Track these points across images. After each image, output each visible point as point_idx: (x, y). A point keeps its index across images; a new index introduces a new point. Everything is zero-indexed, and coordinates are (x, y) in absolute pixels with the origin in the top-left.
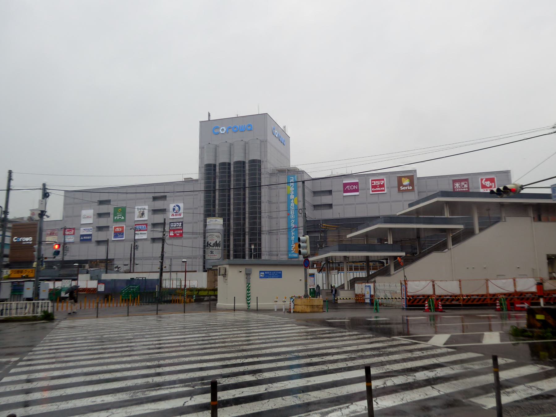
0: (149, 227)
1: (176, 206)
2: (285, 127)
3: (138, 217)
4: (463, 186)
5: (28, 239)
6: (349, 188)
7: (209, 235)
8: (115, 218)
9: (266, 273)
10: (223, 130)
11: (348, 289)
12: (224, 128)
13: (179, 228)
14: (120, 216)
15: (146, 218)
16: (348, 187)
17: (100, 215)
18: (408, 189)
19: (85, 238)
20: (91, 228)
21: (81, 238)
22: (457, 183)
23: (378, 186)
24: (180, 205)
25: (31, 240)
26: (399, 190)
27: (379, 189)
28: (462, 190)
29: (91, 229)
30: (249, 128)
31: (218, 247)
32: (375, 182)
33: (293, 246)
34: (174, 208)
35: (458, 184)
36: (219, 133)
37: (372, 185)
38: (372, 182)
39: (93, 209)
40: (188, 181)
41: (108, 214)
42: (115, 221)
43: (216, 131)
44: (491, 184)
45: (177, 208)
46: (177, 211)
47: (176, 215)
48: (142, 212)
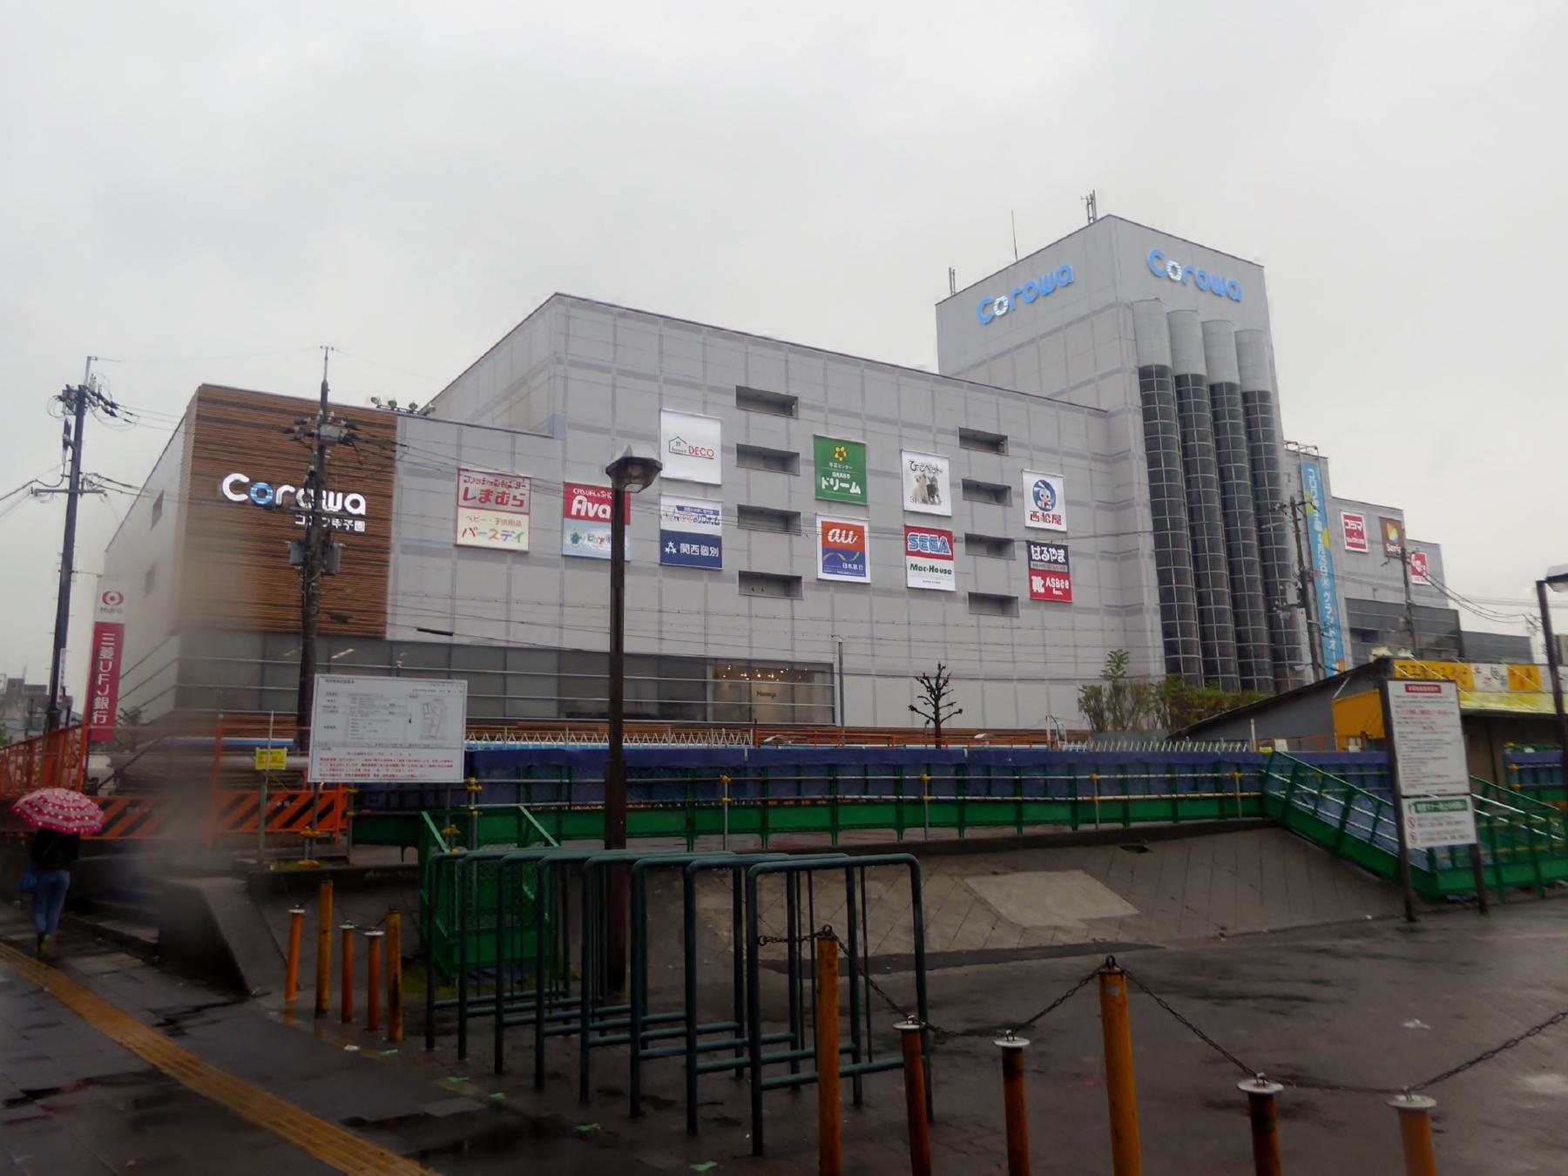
3: (915, 500)
13: (1054, 567)
14: (842, 480)
19: (685, 548)
20: (718, 508)
25: (362, 510)
29: (716, 513)
34: (1036, 489)
42: (827, 498)
46: (1046, 504)
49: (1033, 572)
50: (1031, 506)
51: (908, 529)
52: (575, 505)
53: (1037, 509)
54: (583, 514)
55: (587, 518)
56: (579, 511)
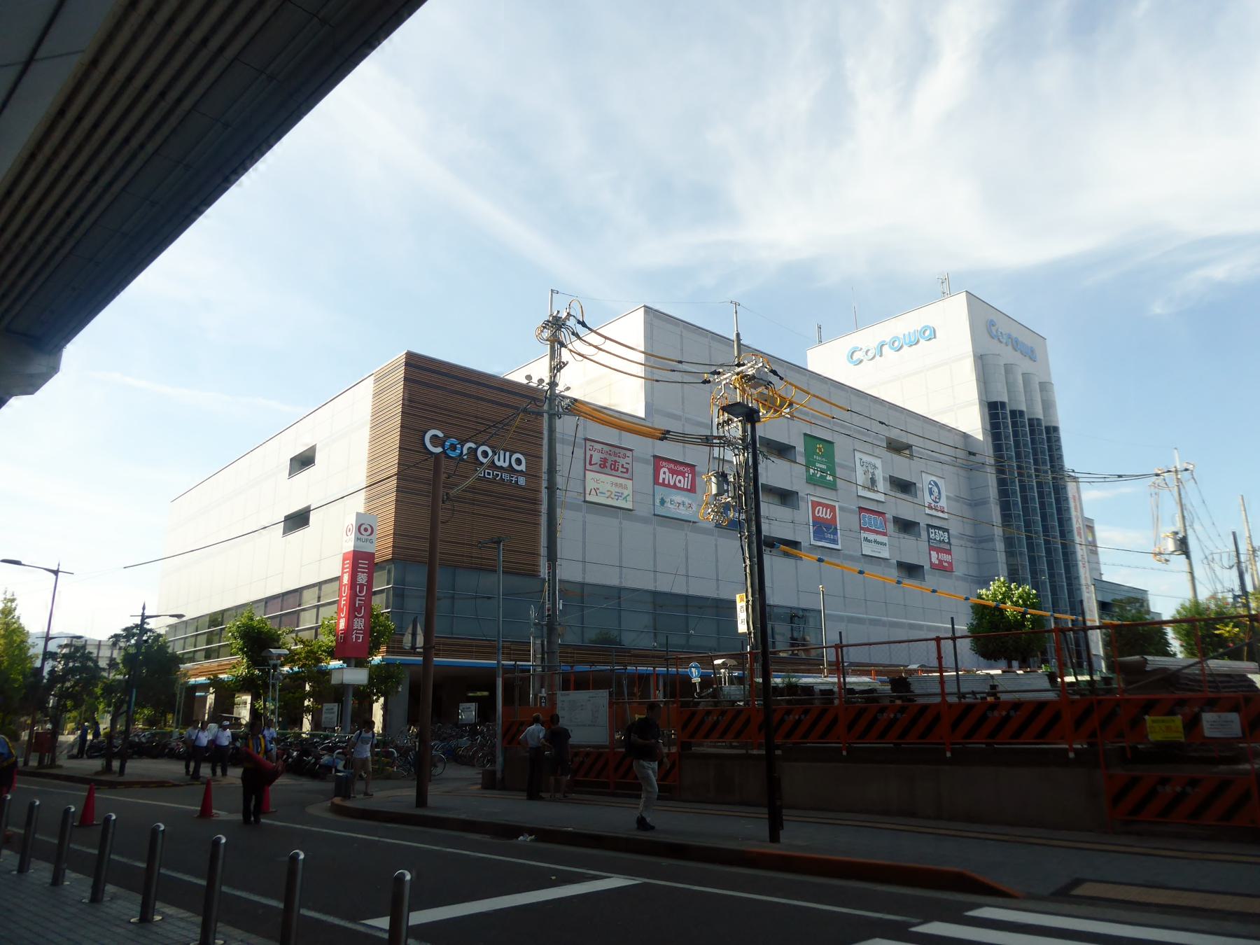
13: (942, 546)
25: (523, 467)
34: (930, 486)
46: (936, 498)
49: (931, 548)
51: (861, 509)
52: (662, 476)
53: (932, 502)
54: (666, 482)
55: (668, 486)
56: (664, 479)
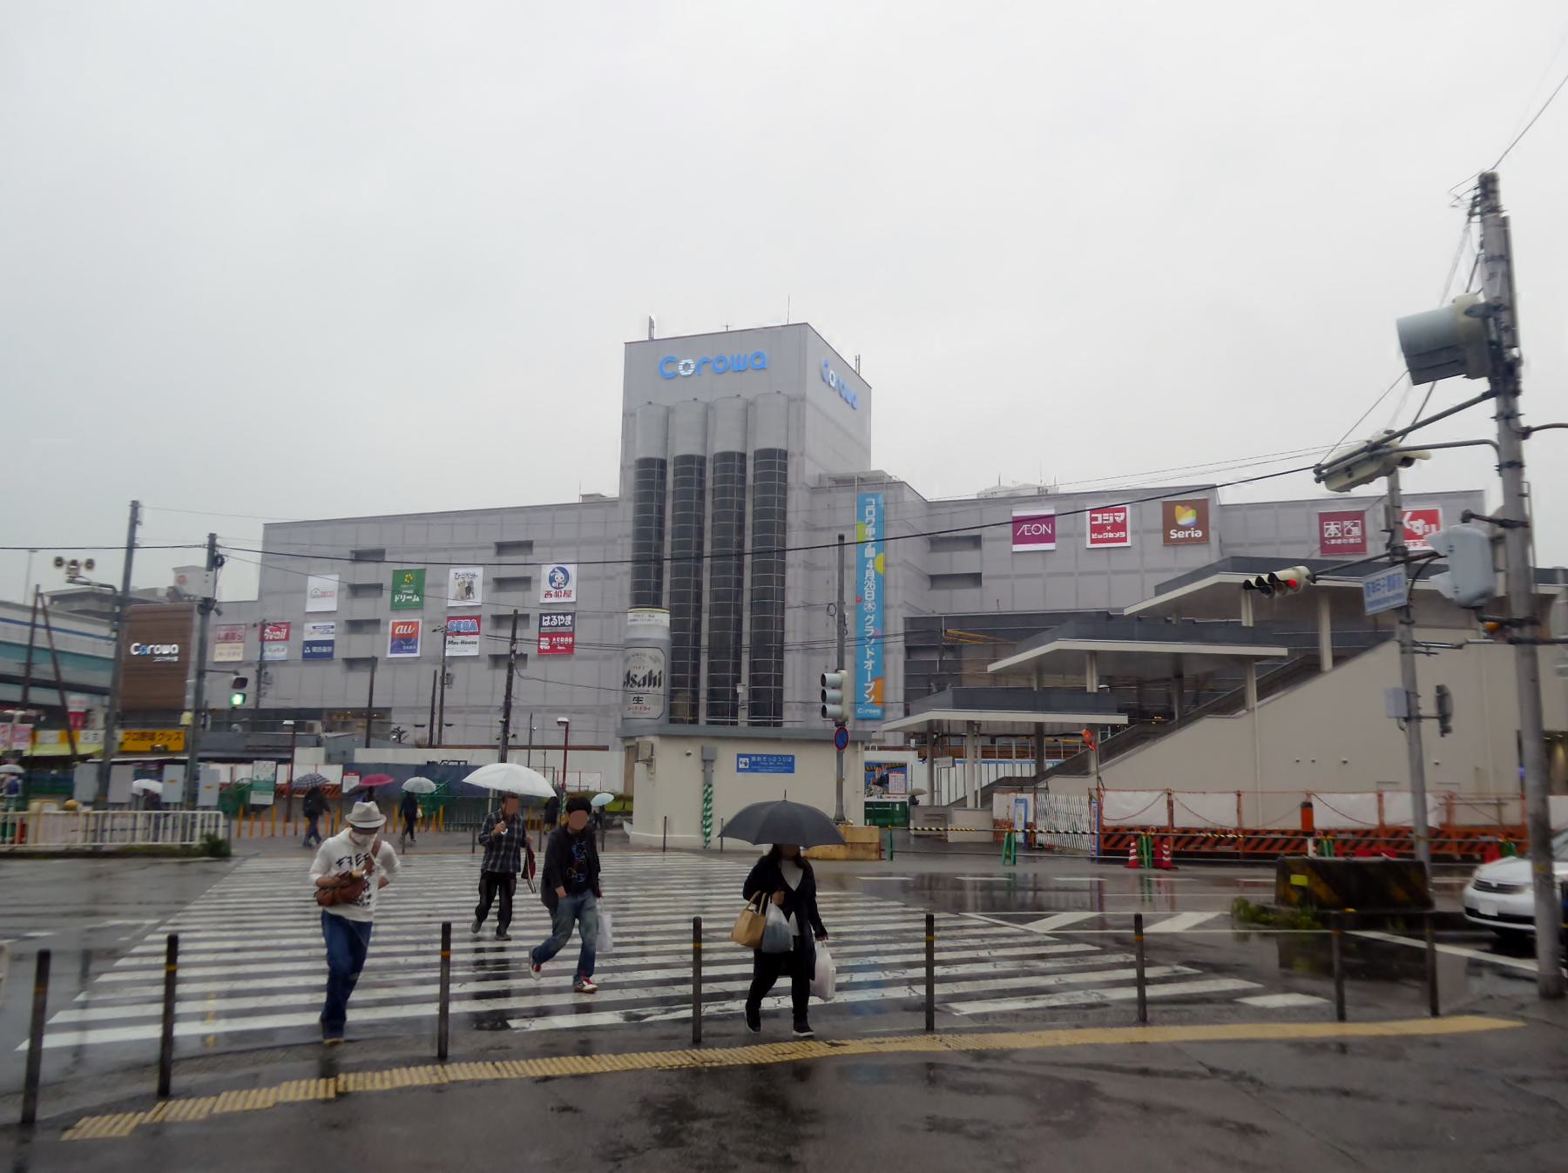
0: (486, 626)
1: (556, 570)
2: (858, 359)
4: (1349, 532)
5: (167, 650)
6: (1029, 531)
7: (633, 656)
8: (396, 599)
9: (754, 759)
10: (686, 366)
11: (976, 806)
12: (690, 361)
14: (408, 595)
15: (477, 598)
16: (1025, 527)
17: (356, 590)
18: (1193, 536)
19: (315, 649)
20: (332, 624)
21: (304, 649)
22: (1332, 523)
23: (1109, 528)
24: (568, 569)
26: (1168, 541)
27: (1111, 535)
28: (1345, 541)
29: (332, 627)
30: (757, 362)
31: (655, 685)
32: (1099, 516)
33: (869, 687)
35: (1335, 524)
36: (677, 375)
37: (1093, 523)
38: (1093, 515)
39: (339, 574)
40: (593, 502)
41: (378, 588)
42: (396, 607)
43: (668, 370)
44: (1427, 526)
45: (560, 576)
47: (557, 595)
48: (467, 585)
50: (545, 586)
53: (551, 589)
